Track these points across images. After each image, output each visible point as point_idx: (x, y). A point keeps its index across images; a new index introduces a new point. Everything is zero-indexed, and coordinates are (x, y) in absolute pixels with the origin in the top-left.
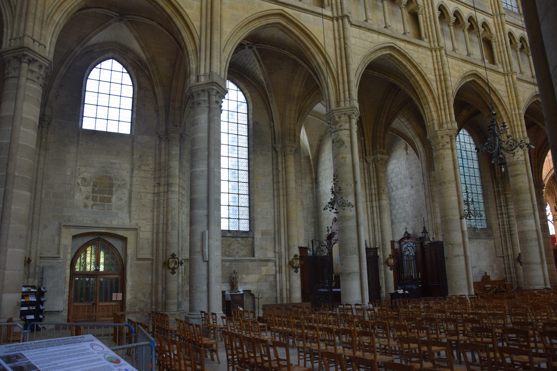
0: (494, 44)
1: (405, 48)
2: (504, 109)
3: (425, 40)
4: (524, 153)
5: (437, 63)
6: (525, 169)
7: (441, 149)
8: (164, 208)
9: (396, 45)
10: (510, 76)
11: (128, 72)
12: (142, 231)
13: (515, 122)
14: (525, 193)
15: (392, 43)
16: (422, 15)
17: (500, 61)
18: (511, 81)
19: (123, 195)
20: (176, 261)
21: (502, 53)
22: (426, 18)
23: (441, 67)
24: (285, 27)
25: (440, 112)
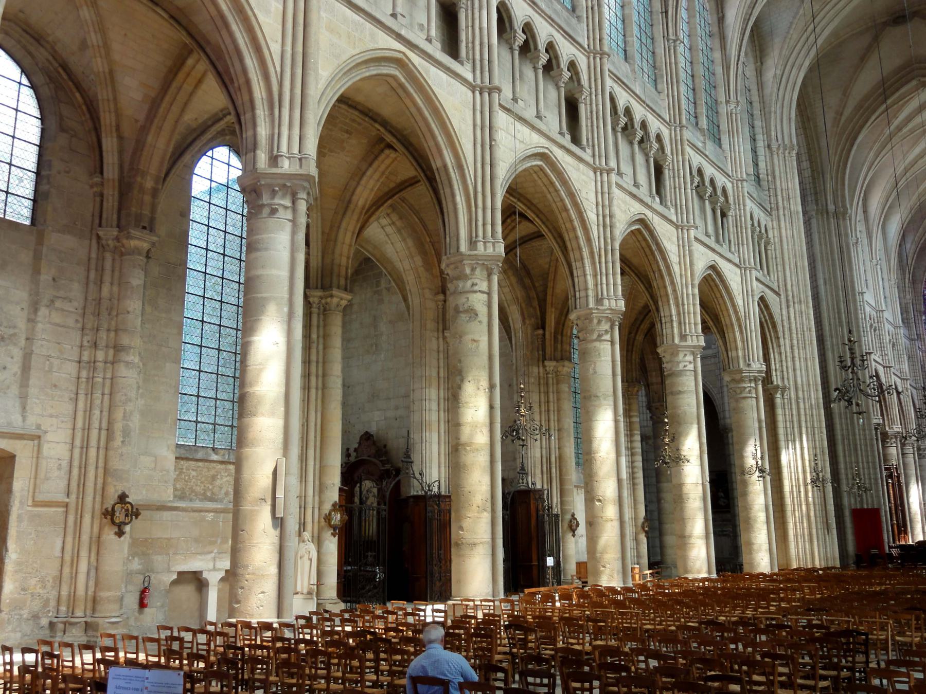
0: (666, 171)
1: (563, 161)
2: (673, 283)
3: (587, 150)
4: (694, 360)
5: (602, 193)
6: (693, 384)
7: (595, 340)
8: (103, 394)
9: (551, 152)
11: (32, 87)
12: (48, 442)
13: (686, 306)
15: (547, 148)
16: (586, 105)
17: (674, 204)
18: (686, 240)
19: (9, 359)
20: (127, 510)
21: (677, 190)
22: (591, 112)
23: (607, 203)
24: (401, 86)
25: (599, 277)
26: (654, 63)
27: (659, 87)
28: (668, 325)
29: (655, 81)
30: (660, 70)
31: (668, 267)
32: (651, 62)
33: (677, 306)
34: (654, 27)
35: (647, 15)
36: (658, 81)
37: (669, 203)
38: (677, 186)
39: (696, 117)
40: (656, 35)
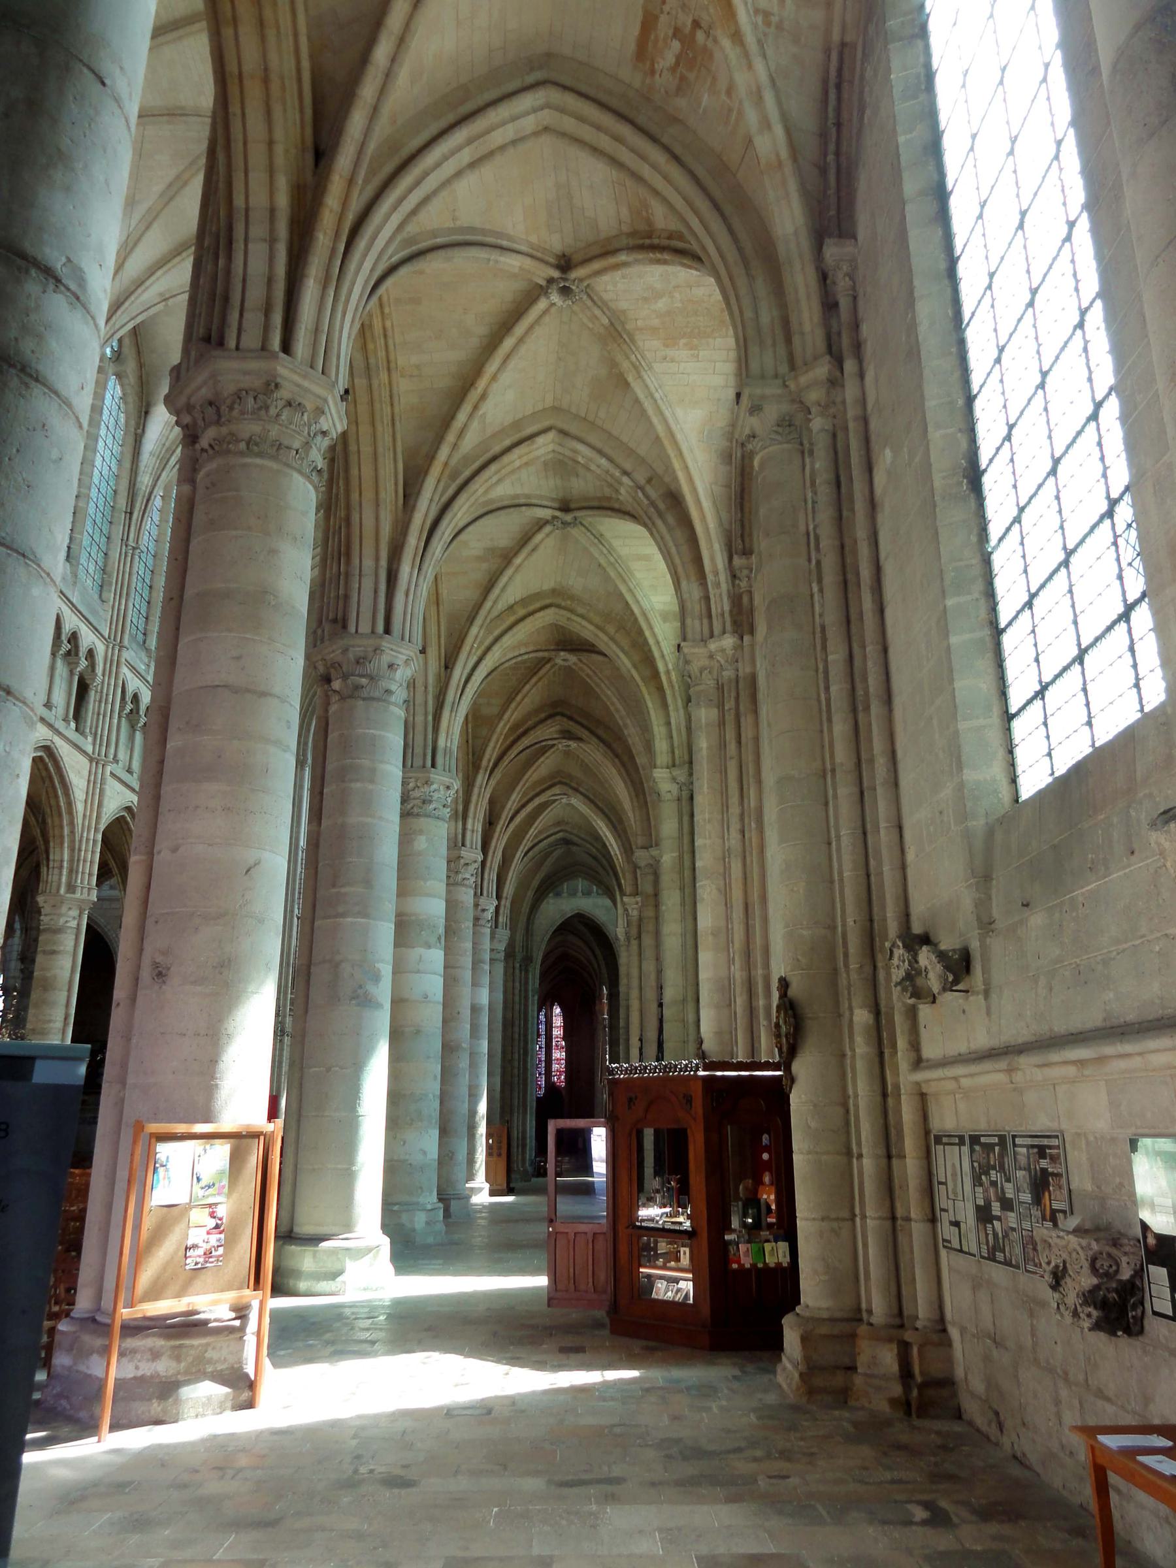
0: (92, 693)
2: (72, 823)
4: (80, 916)
6: (72, 943)
10: (100, 767)
13: (83, 853)
14: (60, 990)
21: (101, 717)
26: (105, 566)
27: (104, 595)
28: (56, 871)
29: (101, 586)
30: (110, 576)
31: (70, 804)
32: (100, 563)
33: (72, 849)
34: (113, 526)
35: (108, 510)
36: (105, 588)
37: (88, 730)
38: (102, 712)
39: (145, 634)
40: (113, 536)
